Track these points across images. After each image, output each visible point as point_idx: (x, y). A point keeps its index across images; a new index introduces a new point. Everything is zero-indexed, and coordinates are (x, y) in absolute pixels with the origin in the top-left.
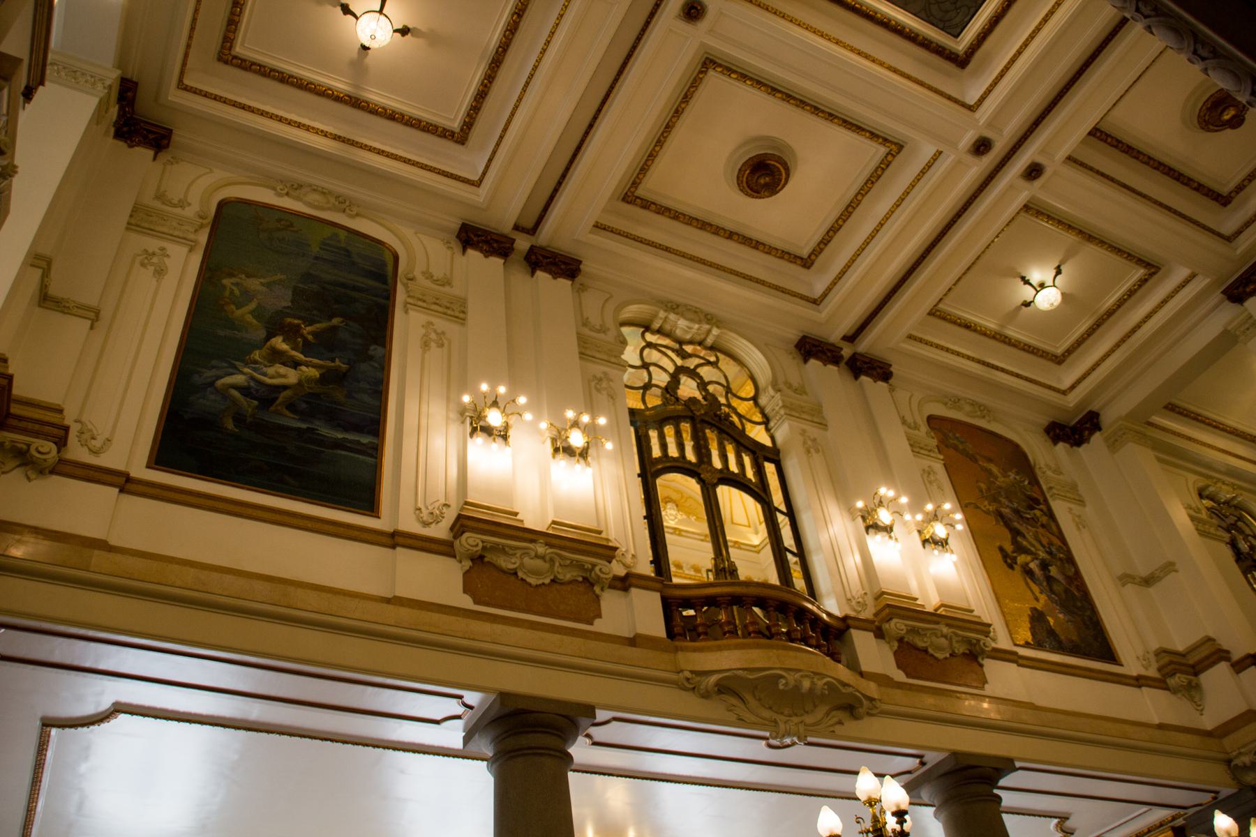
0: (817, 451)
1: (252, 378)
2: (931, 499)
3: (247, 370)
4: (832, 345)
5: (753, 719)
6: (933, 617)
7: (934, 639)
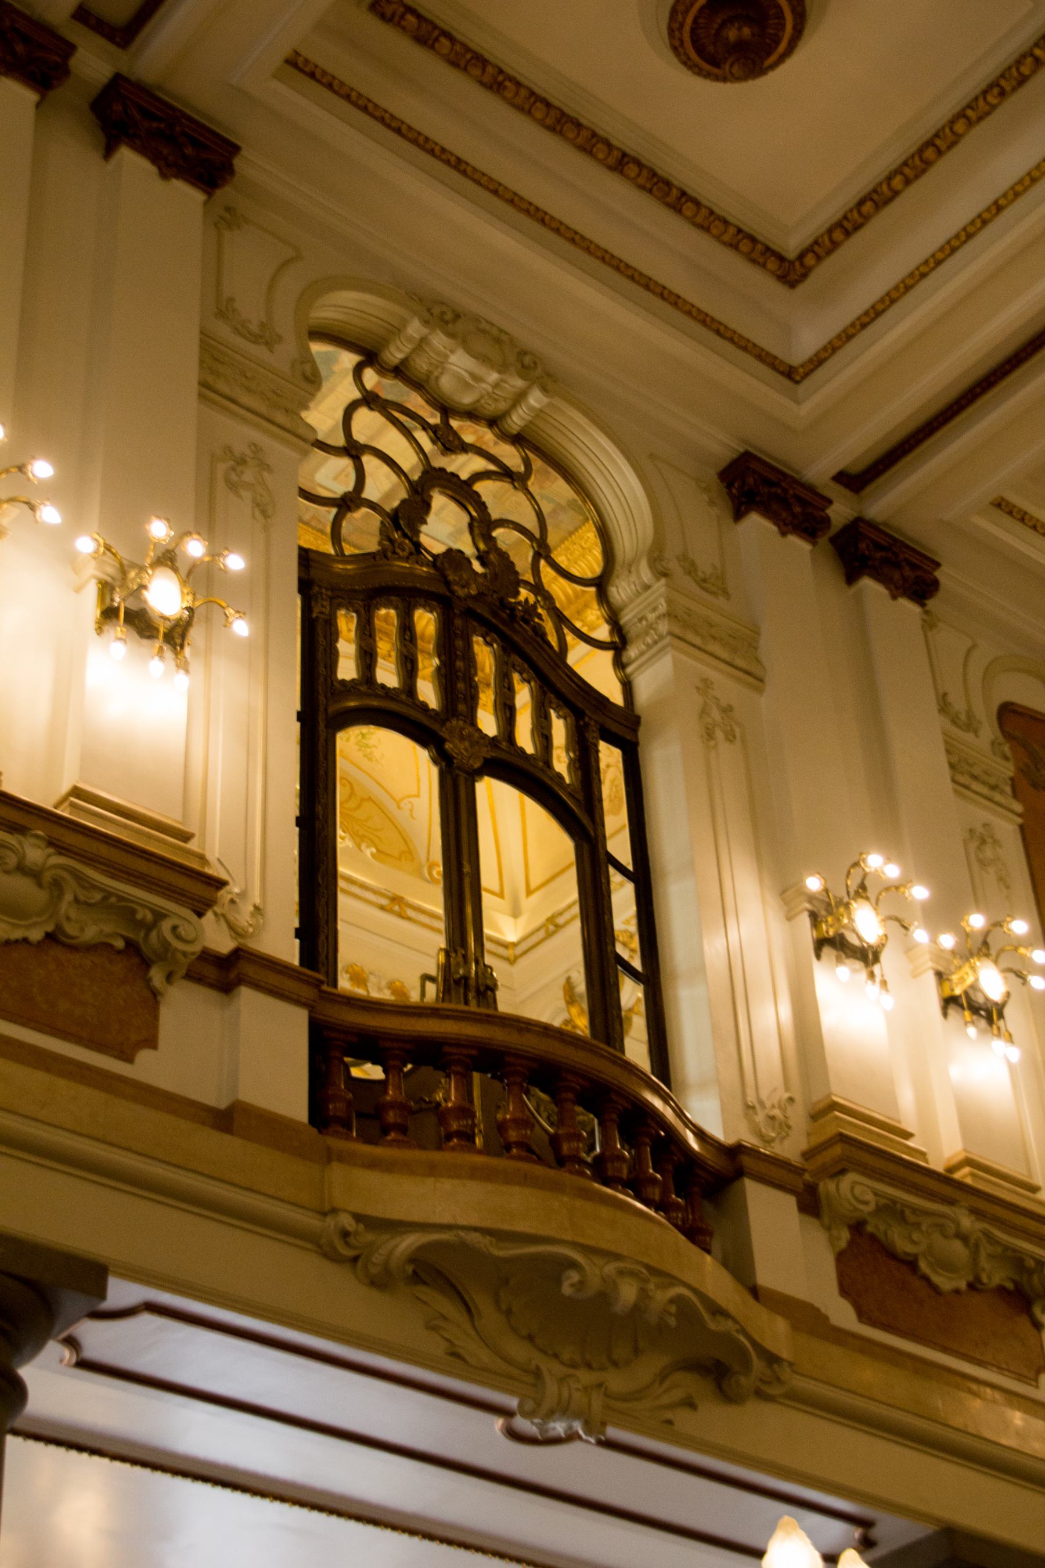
0: (730, 737)
2: (979, 903)
4: (811, 489)
5: (485, 1356)
6: (942, 1186)
7: (937, 1237)
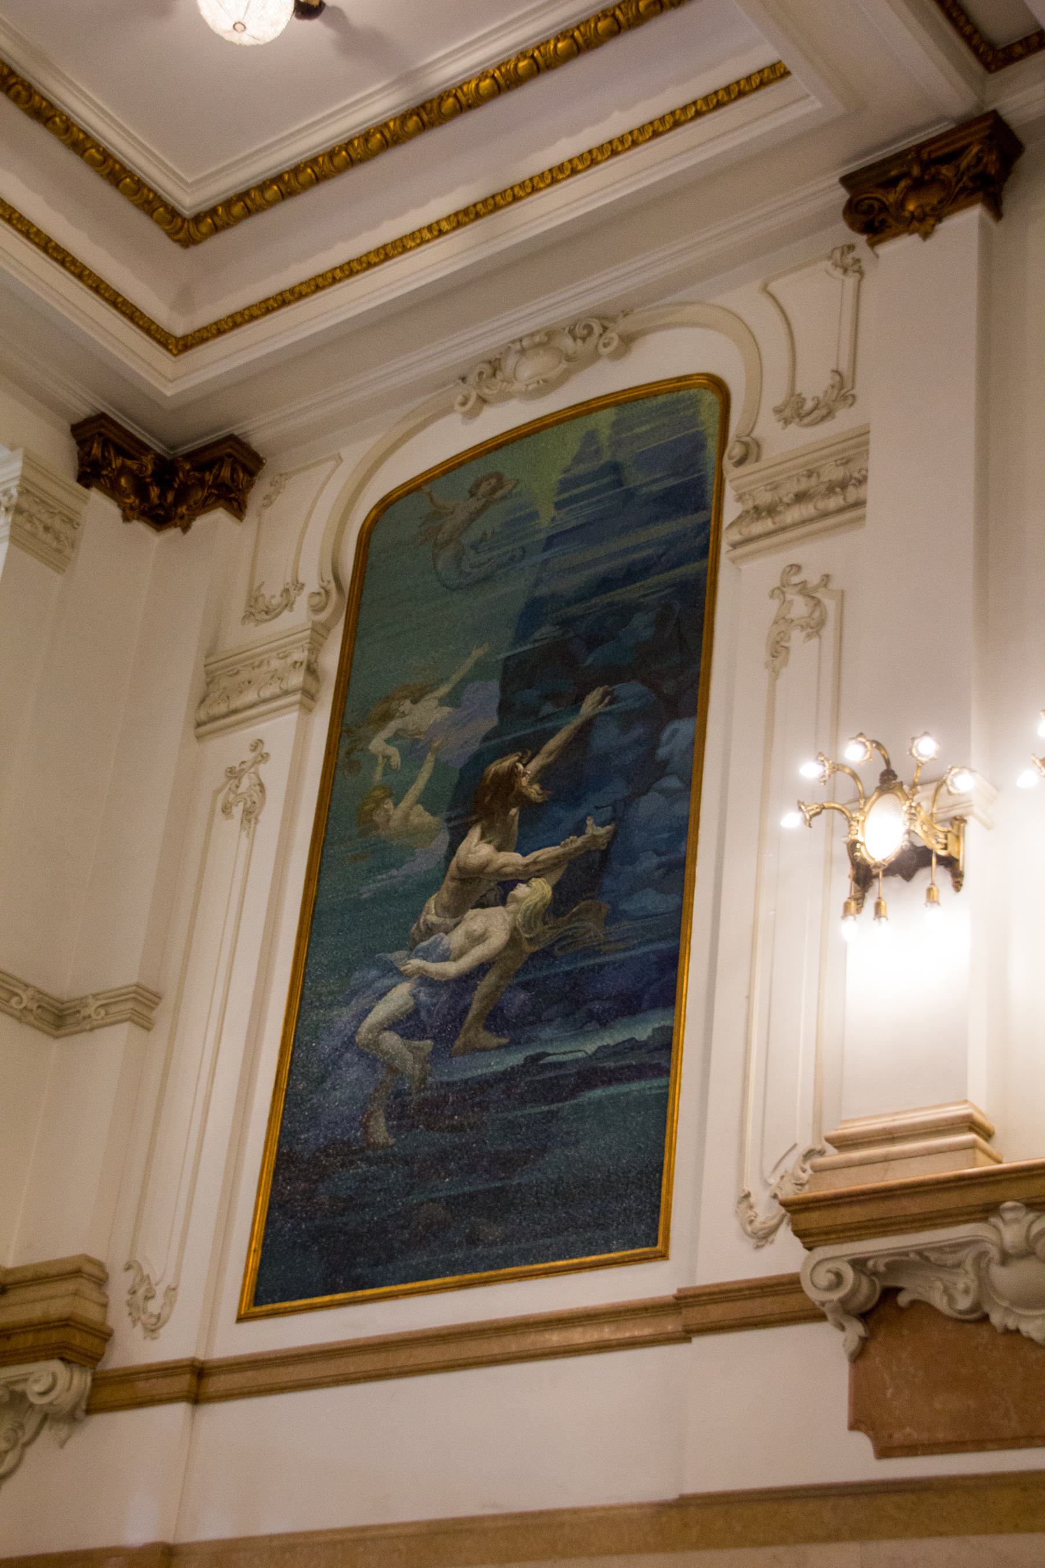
1: (426, 980)
3: (416, 963)
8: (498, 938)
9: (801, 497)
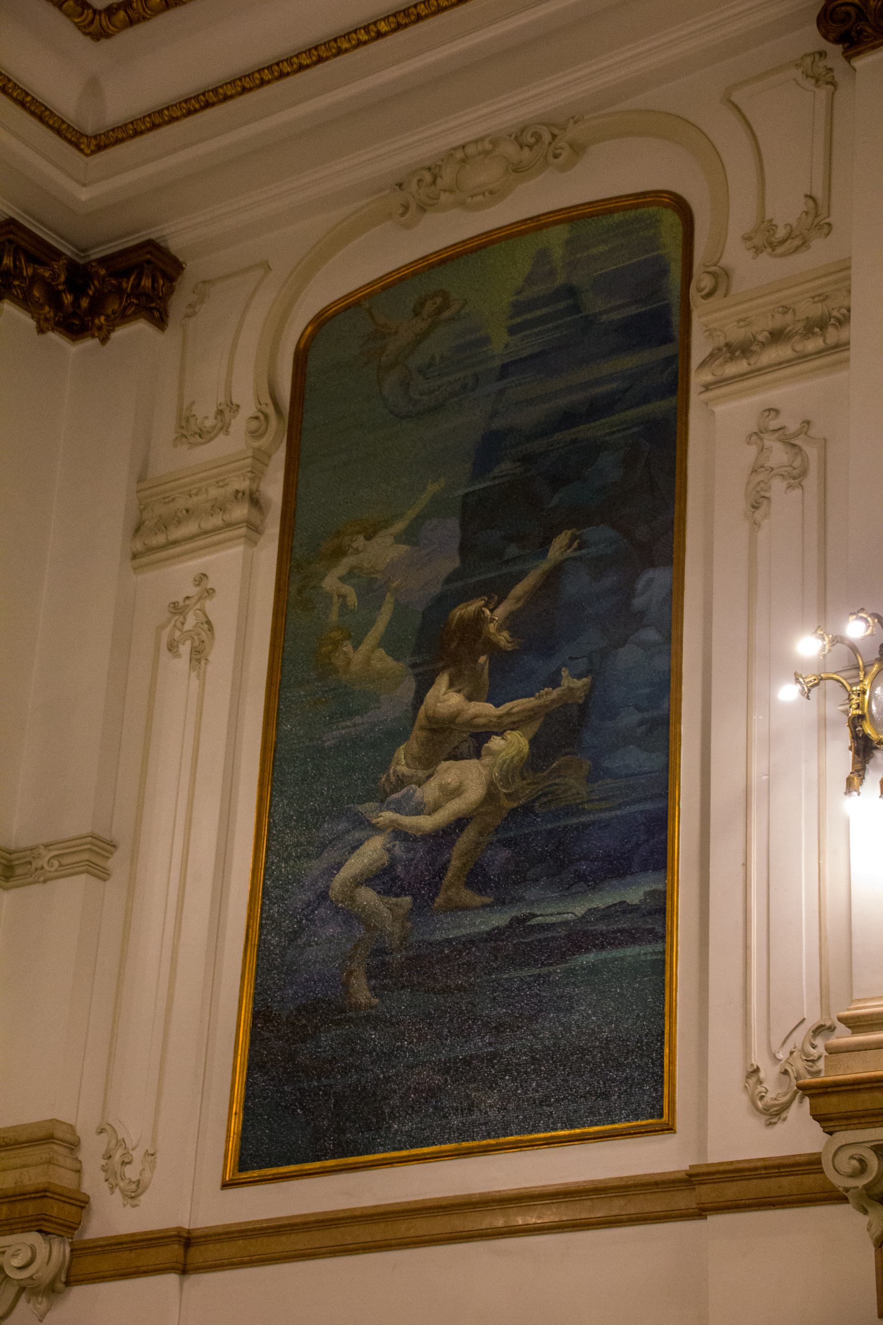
1: (400, 834)
3: (388, 815)
8: (474, 793)
9: (777, 336)
